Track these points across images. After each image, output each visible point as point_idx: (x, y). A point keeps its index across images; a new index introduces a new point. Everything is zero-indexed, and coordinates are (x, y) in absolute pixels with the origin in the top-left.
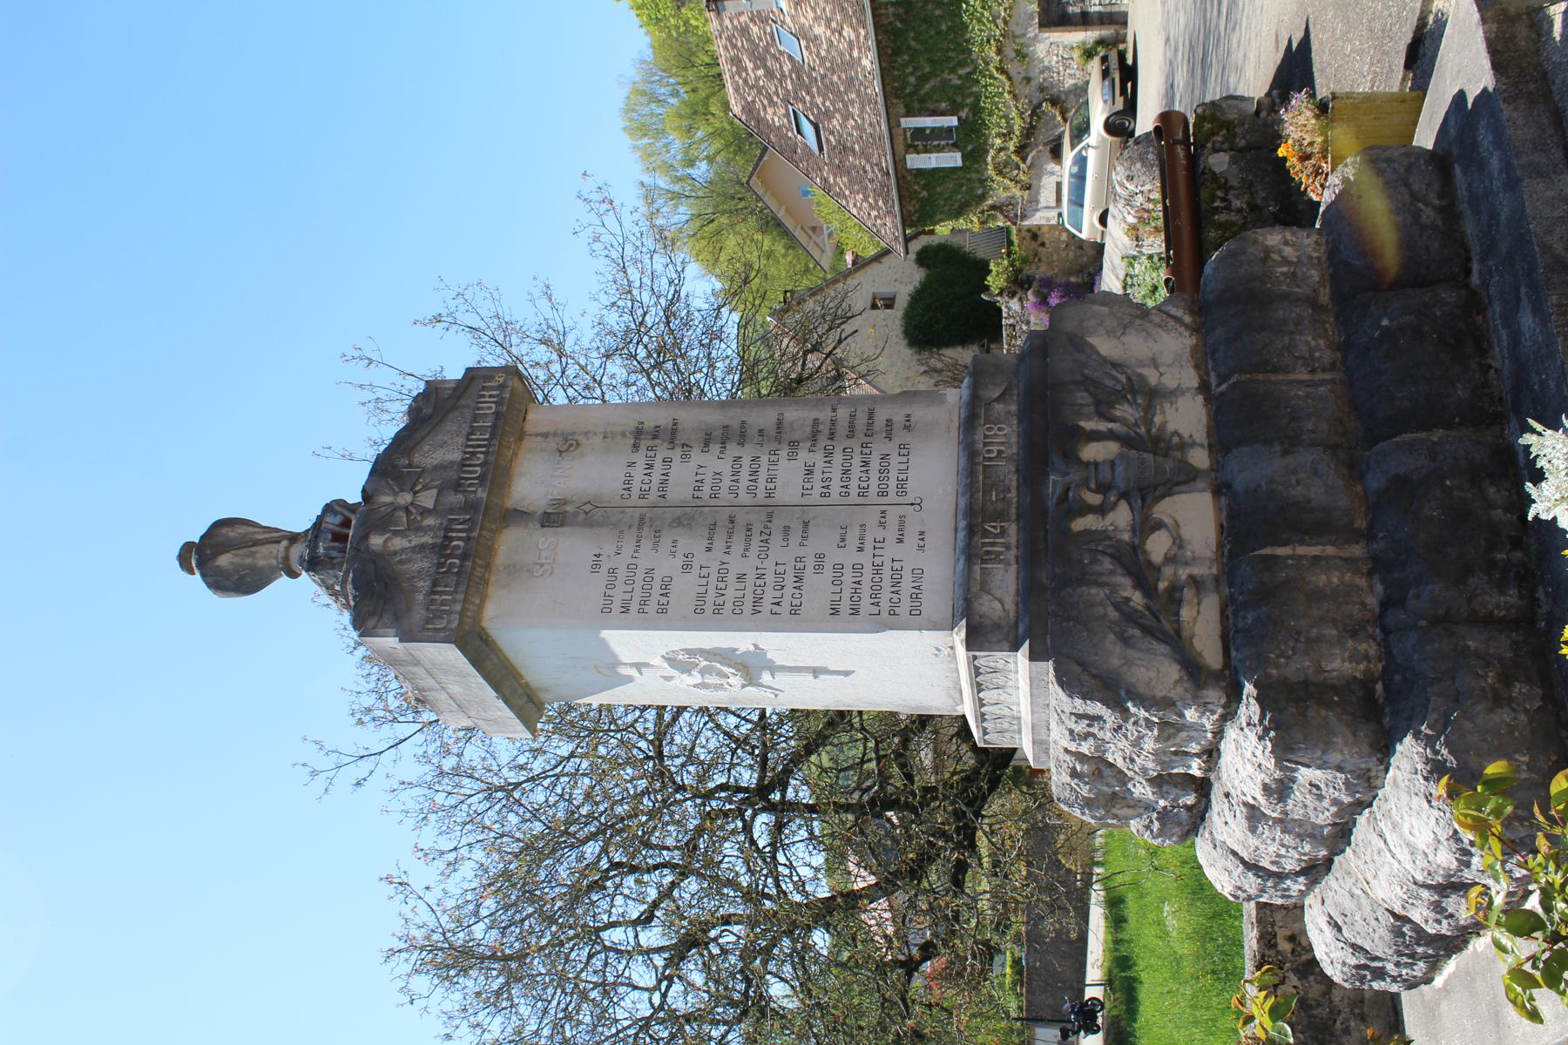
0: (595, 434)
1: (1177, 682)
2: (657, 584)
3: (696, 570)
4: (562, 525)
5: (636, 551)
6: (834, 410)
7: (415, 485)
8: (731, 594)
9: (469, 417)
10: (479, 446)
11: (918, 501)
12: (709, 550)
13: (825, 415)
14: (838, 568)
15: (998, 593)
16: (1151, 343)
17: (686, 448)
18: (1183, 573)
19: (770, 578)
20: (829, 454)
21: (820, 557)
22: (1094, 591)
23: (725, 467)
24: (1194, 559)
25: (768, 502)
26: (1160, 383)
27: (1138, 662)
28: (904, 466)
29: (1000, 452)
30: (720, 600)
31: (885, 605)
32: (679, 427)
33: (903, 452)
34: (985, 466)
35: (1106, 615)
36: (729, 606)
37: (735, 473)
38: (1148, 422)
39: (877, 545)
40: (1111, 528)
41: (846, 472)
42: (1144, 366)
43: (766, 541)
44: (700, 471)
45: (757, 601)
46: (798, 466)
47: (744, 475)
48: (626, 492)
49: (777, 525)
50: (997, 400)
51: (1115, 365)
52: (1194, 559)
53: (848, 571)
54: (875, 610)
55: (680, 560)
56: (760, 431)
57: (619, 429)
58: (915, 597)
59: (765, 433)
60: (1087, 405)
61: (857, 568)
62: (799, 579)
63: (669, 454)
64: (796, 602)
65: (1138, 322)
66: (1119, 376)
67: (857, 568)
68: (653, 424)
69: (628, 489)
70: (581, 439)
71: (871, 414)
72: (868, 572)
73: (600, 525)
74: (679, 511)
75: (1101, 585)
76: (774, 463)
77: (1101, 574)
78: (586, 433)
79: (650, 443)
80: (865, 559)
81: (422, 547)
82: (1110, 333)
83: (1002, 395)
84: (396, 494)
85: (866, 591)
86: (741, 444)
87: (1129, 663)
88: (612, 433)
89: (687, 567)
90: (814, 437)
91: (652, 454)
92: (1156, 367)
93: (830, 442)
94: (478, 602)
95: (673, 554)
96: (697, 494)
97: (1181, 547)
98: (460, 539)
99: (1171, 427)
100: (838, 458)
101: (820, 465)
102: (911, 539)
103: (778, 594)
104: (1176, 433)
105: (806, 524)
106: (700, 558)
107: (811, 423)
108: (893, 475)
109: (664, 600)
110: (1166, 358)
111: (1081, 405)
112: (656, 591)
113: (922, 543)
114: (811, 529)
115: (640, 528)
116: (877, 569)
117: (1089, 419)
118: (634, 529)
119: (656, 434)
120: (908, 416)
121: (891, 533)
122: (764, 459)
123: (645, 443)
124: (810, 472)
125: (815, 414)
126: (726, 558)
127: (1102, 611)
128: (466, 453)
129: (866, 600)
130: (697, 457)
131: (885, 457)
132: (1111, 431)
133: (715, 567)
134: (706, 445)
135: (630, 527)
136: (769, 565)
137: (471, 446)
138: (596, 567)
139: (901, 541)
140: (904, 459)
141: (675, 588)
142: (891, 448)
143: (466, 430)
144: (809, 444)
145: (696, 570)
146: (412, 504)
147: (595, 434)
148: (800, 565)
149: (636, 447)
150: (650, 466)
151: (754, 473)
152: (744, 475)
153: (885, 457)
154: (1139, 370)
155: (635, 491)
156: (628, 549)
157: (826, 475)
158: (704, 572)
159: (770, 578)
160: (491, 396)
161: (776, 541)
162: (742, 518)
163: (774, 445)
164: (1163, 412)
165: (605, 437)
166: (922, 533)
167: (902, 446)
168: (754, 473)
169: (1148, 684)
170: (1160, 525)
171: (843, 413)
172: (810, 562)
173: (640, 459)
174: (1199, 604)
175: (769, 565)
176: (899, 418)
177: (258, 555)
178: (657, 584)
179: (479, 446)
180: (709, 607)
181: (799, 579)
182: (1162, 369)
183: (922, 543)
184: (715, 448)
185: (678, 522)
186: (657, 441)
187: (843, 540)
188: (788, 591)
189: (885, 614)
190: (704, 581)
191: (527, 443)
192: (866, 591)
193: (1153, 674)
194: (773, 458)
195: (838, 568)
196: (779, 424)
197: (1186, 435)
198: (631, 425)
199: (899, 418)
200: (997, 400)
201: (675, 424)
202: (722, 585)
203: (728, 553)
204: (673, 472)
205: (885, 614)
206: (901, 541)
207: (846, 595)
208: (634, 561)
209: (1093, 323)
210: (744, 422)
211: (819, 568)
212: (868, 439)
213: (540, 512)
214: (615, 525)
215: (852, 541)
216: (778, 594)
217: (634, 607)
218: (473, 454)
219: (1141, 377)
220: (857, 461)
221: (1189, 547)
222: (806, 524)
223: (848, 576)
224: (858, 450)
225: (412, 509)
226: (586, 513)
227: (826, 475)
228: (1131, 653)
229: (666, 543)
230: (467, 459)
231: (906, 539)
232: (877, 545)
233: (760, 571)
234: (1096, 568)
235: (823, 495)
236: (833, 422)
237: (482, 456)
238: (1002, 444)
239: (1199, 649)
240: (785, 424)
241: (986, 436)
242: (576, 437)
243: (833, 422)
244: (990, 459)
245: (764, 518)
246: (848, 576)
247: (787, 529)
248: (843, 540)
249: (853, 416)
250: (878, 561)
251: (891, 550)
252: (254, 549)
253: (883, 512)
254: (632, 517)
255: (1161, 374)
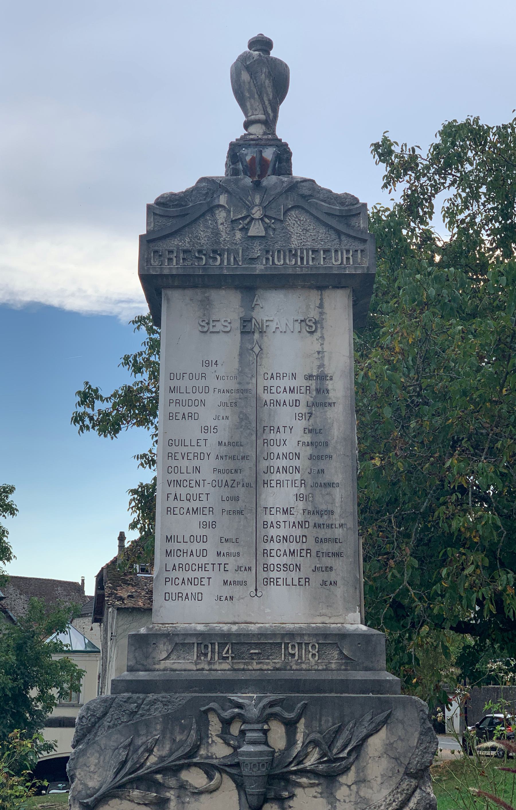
0: (322, 344)
1: (85, 785)
2: (193, 410)
3: (203, 436)
4: (242, 333)
5: (219, 391)
6: (341, 526)
7: (270, 218)
8: (184, 463)
9: (327, 247)
10: (302, 259)
11: (259, 594)
12: (220, 444)
13: (337, 520)
14: (204, 539)
15: (173, 656)
16: (379, 780)
17: (308, 416)
18: (171, 794)
19: (196, 490)
20: (301, 525)
21: (213, 525)
22: (159, 727)
23: (291, 447)
24: (183, 803)
25: (260, 482)
26: (341, 785)
27: (102, 758)
28: (289, 582)
29: (293, 655)
30: (179, 456)
31: (173, 575)
32: (328, 409)
33: (303, 582)
34: (281, 643)
35: (139, 735)
36: (174, 463)
37: (285, 456)
38: (303, 772)
39: (222, 566)
40: (210, 741)
41: (285, 539)
42: (357, 772)
43: (227, 484)
44: (287, 429)
45: (178, 483)
46: (291, 501)
47: (284, 463)
48: (269, 376)
49: (240, 491)
50: (341, 653)
51: (358, 748)
52: (183, 803)
53: (202, 546)
54: (170, 567)
55: (211, 423)
56: (323, 471)
57: (326, 362)
58: (179, 596)
59: (320, 475)
60: (320, 725)
61: (203, 553)
62: (195, 511)
63: (303, 403)
64: (177, 511)
65: (402, 770)
66: (346, 751)
67: (203, 553)
68: (330, 387)
69: (272, 377)
70: (318, 334)
71: (337, 555)
72: (203, 561)
73: (240, 362)
74: (253, 417)
75: (163, 732)
76: (293, 482)
77: (172, 733)
78: (322, 337)
79: (313, 387)
80: (211, 558)
81: (217, 233)
82: (389, 747)
83: (346, 657)
84: (260, 204)
85: (184, 560)
86: (311, 458)
87: (102, 751)
88: (323, 357)
89: (206, 429)
90: (320, 513)
91: (303, 390)
92: (355, 783)
93: (312, 524)
94: (176, 284)
95: (217, 418)
96: (267, 429)
97: (194, 793)
98: (222, 261)
99: (298, 791)
100: (298, 532)
101: (292, 519)
102: (227, 591)
103: (183, 497)
104: (292, 796)
105: (241, 512)
106: (213, 438)
107: (330, 508)
108: (282, 575)
109: (180, 416)
110: (365, 792)
111: (320, 720)
112: (187, 410)
113: (223, 598)
114: (237, 517)
115: (238, 391)
116: (202, 567)
117: (306, 727)
118: (237, 386)
119: (321, 391)
120: (335, 583)
121: (229, 577)
122: (298, 476)
123: (313, 384)
124: (285, 512)
125: (338, 511)
126: (213, 457)
127: (143, 732)
128: (296, 251)
129: (176, 560)
130: (300, 425)
131: (298, 567)
132: (295, 743)
133: (206, 450)
134: (310, 431)
135: (240, 383)
136: (208, 489)
137: (302, 253)
138: (207, 364)
139: (225, 583)
140: (296, 582)
141: (191, 423)
142: (306, 571)
143: (317, 246)
144: (310, 509)
145: (203, 436)
146: (253, 219)
147: (322, 344)
148: (206, 511)
149: (309, 377)
150: (292, 391)
151: (285, 470)
152: (284, 463)
153: (298, 567)
154: (353, 768)
155: (270, 383)
156: (220, 385)
157: (282, 524)
158: (202, 443)
159: (196, 490)
160: (348, 259)
161: (226, 492)
162: (247, 465)
163: (310, 482)
164: (312, 785)
165: (319, 352)
166: (231, 598)
167: (307, 580)
168: (285, 470)
169: (85, 765)
170: (210, 778)
171: (339, 533)
172: (209, 518)
173: (300, 382)
174: (145, 804)
175: (208, 489)
176: (333, 576)
177: (252, 101)
178: (193, 410)
179: (302, 259)
180: (173, 449)
181: (195, 511)
182: (354, 787)
183: (223, 598)
184: (307, 438)
185: (244, 418)
186: (314, 393)
187: (227, 541)
188: (186, 505)
189: (166, 574)
190: (194, 443)
191: (320, 292)
192: (184, 560)
193: (92, 768)
194: (298, 483)
195: (204, 539)
196: (330, 485)
197: (291, 803)
198: (329, 371)
199: (333, 576)
200: (341, 653)
201: (330, 404)
202: (191, 456)
203: (217, 457)
204: (287, 409)
205: (166, 574)
206: (225, 583)
207: (182, 546)
208: (211, 390)
209: (400, 732)
210: (331, 457)
211: (204, 525)
212: (314, 554)
213: (254, 314)
214: (241, 372)
215: (225, 548)
216: (183, 497)
217: (174, 396)
218: (295, 255)
219: (346, 770)
220: (294, 546)
221: (193, 800)
222: (241, 512)
223: (196, 547)
224: (305, 546)
225: (248, 220)
226: (252, 349)
227: (282, 524)
228: (109, 752)
229: (227, 412)
230: (290, 251)
231: (227, 587)
232: (222, 566)
233: (202, 482)
234: (177, 729)
235: (265, 524)
236: (330, 526)
237: (293, 262)
238: (300, 657)
239: (110, 802)
240: (329, 490)
241: (307, 644)
242: (319, 330)
243: (330, 526)
244: (286, 648)
245: (246, 481)
246: (196, 547)
247: (237, 499)
248: (227, 541)
249: (335, 541)
250: (209, 567)
251: (217, 577)
252: (256, 96)
253: (250, 569)
254: (248, 383)
255: (349, 786)
